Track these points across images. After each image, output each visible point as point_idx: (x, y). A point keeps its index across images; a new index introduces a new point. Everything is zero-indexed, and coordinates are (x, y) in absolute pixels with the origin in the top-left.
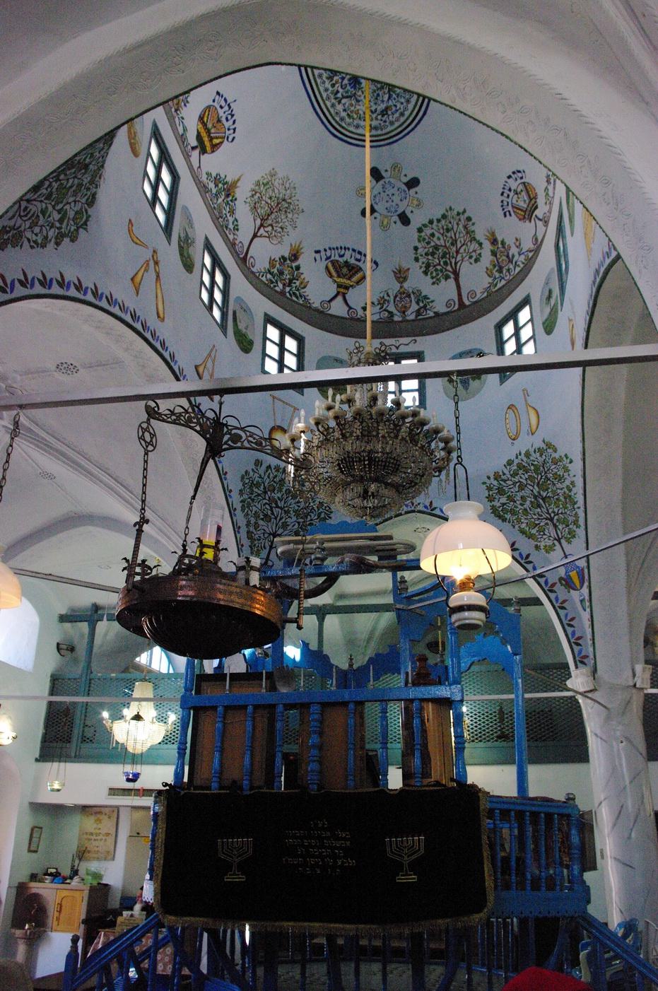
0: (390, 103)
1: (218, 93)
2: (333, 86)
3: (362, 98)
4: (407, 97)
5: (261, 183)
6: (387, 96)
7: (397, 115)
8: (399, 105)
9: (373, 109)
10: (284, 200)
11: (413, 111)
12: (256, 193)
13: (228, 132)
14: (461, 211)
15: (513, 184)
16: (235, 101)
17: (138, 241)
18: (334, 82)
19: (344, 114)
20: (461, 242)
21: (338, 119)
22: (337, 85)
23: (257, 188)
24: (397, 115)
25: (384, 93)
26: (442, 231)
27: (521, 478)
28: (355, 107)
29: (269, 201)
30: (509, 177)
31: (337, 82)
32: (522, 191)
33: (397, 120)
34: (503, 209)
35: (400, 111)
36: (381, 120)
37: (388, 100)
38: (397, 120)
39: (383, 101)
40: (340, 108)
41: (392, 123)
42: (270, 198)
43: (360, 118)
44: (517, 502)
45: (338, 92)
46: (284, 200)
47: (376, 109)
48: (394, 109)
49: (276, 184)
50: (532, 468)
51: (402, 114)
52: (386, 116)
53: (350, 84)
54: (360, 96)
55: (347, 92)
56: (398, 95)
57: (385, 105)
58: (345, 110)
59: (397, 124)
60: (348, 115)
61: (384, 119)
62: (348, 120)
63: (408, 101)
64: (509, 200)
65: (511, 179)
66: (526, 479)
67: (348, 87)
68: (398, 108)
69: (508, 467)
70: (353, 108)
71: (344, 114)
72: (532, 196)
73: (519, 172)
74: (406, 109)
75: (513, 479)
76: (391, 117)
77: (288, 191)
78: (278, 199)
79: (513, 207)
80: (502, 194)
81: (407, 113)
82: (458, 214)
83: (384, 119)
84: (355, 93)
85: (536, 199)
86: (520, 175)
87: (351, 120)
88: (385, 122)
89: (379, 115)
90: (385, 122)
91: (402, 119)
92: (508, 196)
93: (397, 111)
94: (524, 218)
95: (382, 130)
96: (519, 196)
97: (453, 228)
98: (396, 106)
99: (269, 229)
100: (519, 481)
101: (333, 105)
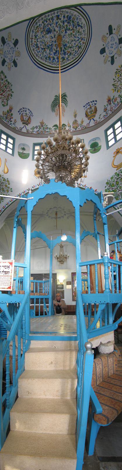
0: (41, 49)
2: (49, 20)
3: (43, 35)
4: (43, 58)
6: (43, 47)
8: (39, 53)
11: (35, 58)
14: (12, 91)
18: (50, 20)
19: (38, 25)
20: (5, 94)
21: (37, 21)
25: (44, 46)
26: (4, 84)
28: (40, 31)
31: (50, 22)
33: (35, 53)
37: (41, 48)
38: (35, 53)
40: (41, 23)
43: (36, 33)
45: (47, 22)
47: (38, 41)
51: (37, 55)
53: (48, 28)
54: (43, 34)
55: (46, 27)
56: (43, 53)
57: (40, 46)
59: (33, 52)
61: (35, 46)
62: (36, 26)
63: (41, 58)
67: (47, 27)
71: (38, 25)
81: (37, 58)
82: (11, 90)
83: (35, 46)
84: (45, 31)
87: (35, 28)
89: (36, 42)
90: (34, 46)
91: (35, 55)
93: (38, 53)
95: (31, 44)
97: (7, 89)
101: (42, 19)
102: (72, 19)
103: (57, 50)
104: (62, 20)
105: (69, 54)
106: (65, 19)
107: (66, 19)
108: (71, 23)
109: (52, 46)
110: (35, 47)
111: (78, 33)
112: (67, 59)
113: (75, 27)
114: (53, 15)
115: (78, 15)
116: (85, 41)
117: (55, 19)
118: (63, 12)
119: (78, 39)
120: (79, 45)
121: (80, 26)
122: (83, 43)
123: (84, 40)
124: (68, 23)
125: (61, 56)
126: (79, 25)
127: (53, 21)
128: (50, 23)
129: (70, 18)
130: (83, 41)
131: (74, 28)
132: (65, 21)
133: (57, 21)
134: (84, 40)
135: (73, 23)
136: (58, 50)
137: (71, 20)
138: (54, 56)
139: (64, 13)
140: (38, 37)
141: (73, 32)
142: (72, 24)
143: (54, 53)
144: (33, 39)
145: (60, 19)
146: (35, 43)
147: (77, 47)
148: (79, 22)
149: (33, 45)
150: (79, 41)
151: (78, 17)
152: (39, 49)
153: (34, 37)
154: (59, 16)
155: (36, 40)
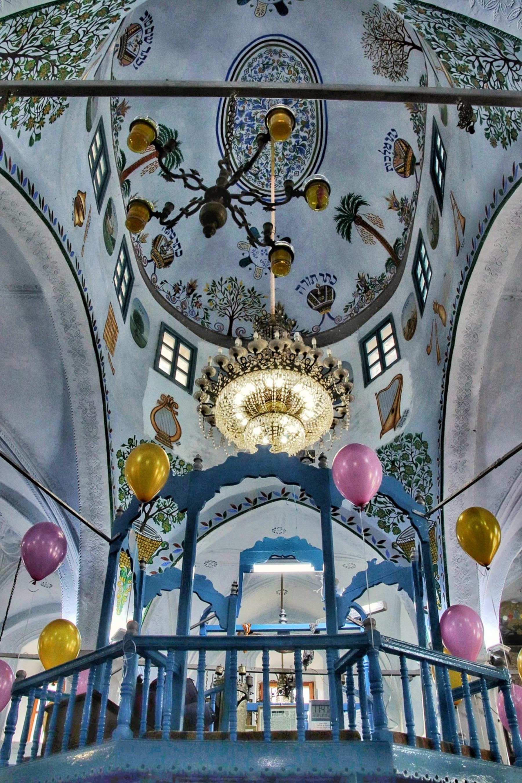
0: (260, 75)
1: (388, 170)
2: (305, 104)
5: (389, 74)
7: (255, 64)
8: (253, 74)
9: (275, 71)
10: (376, 38)
12: (397, 73)
13: (395, 139)
15: (144, 46)
16: (380, 151)
17: (434, 330)
18: (304, 106)
19: (302, 75)
21: (307, 73)
22: (302, 102)
23: (394, 75)
24: (255, 64)
27: (80, 45)
29: (389, 52)
30: (149, 48)
32: (135, 50)
34: (149, 16)
35: (252, 68)
36: (270, 59)
39: (266, 77)
41: (260, 56)
42: (387, 53)
43: (289, 66)
44: (74, 20)
46: (376, 38)
47: (273, 70)
48: (257, 70)
49: (377, 60)
50: (69, 69)
52: (265, 63)
57: (265, 73)
58: (300, 79)
60: (298, 73)
62: (299, 69)
64: (144, 29)
65: (146, 50)
66: (72, 51)
68: (253, 71)
69: (101, 37)
70: (293, 77)
71: (302, 75)
72: (126, 57)
73: (142, 62)
74: (246, 71)
75: (92, 34)
76: (261, 62)
77: (370, 42)
78: (381, 45)
79: (141, 27)
80: (152, 28)
81: (245, 67)
83: (267, 60)
85: (121, 60)
86: (139, 62)
87: (296, 67)
88: (266, 58)
89: (272, 65)
90: (266, 58)
91: (250, 60)
92: (146, 33)
93: (254, 68)
94: (127, 33)
96: (136, 43)
98: (255, 73)
99: (399, 30)
100: (81, 41)
102: (299, 155)
103: (255, 122)
104: (300, 132)
105: (247, 152)
106: (301, 140)
107: (301, 142)
108: (293, 154)
109: (261, 108)
110: (264, 59)
111: (278, 169)
112: (240, 149)
113: (287, 162)
114: (310, 113)
115: (303, 169)
116: (265, 188)
117: (304, 118)
118: (313, 136)
119: (269, 169)
120: (260, 175)
121: (288, 172)
122: (263, 184)
123: (267, 185)
124: (294, 146)
125: (244, 132)
126: (289, 170)
127: (301, 111)
128: (299, 105)
129: (302, 152)
130: (266, 182)
131: (285, 161)
132: (298, 139)
133: (300, 123)
134: (267, 185)
135: (293, 158)
136: (254, 124)
137: (298, 154)
138: (246, 113)
139: (310, 138)
140: (280, 69)
141: (280, 158)
142: (292, 156)
143: (251, 113)
144: (280, 56)
145: (302, 129)
146: (271, 62)
147: (257, 170)
148: (294, 171)
149: (269, 55)
150: (266, 175)
151: (302, 167)
152: (260, 72)
153: (282, 59)
154: (308, 127)
155: (275, 64)
